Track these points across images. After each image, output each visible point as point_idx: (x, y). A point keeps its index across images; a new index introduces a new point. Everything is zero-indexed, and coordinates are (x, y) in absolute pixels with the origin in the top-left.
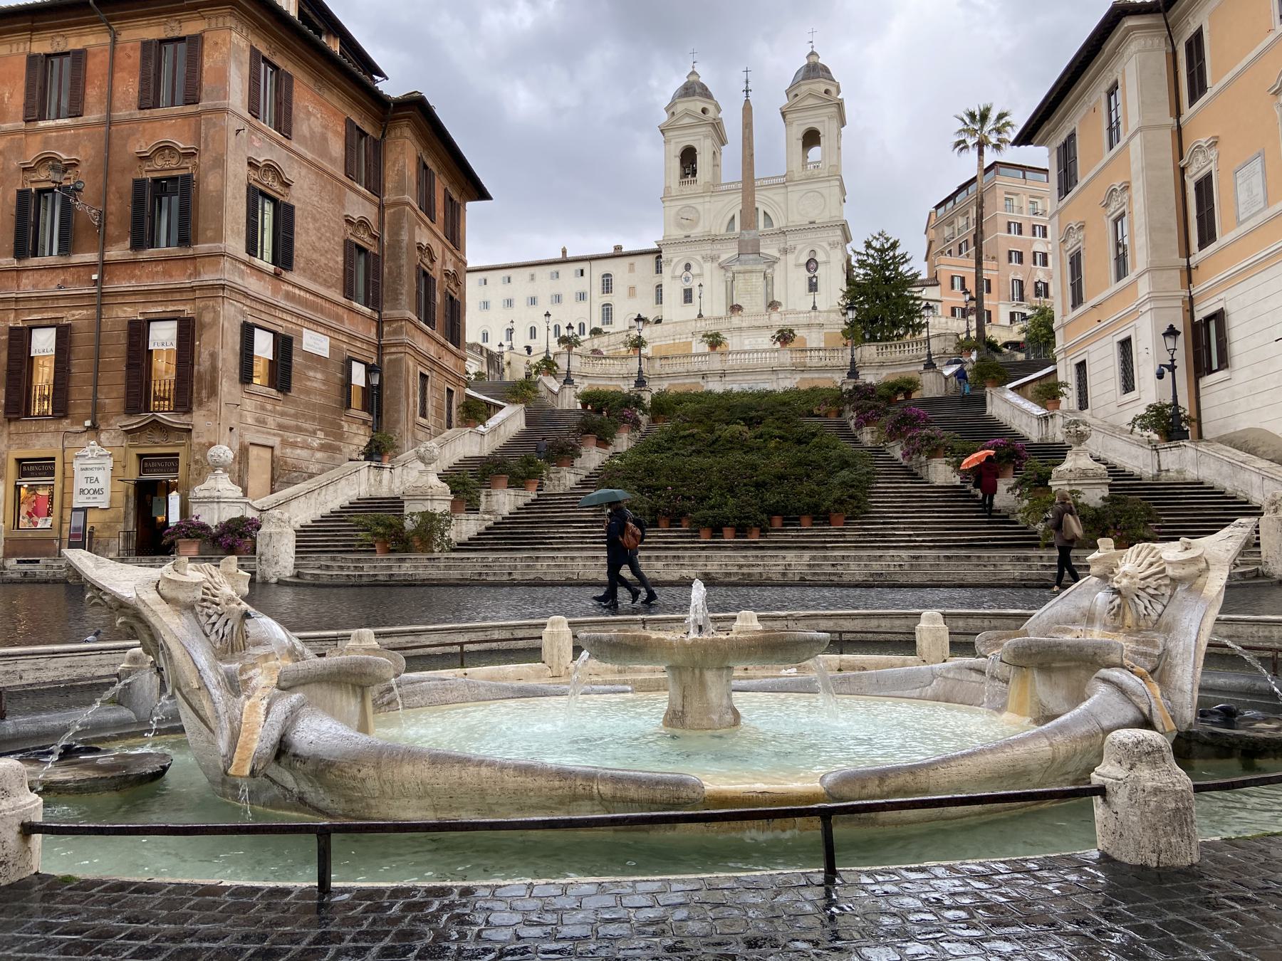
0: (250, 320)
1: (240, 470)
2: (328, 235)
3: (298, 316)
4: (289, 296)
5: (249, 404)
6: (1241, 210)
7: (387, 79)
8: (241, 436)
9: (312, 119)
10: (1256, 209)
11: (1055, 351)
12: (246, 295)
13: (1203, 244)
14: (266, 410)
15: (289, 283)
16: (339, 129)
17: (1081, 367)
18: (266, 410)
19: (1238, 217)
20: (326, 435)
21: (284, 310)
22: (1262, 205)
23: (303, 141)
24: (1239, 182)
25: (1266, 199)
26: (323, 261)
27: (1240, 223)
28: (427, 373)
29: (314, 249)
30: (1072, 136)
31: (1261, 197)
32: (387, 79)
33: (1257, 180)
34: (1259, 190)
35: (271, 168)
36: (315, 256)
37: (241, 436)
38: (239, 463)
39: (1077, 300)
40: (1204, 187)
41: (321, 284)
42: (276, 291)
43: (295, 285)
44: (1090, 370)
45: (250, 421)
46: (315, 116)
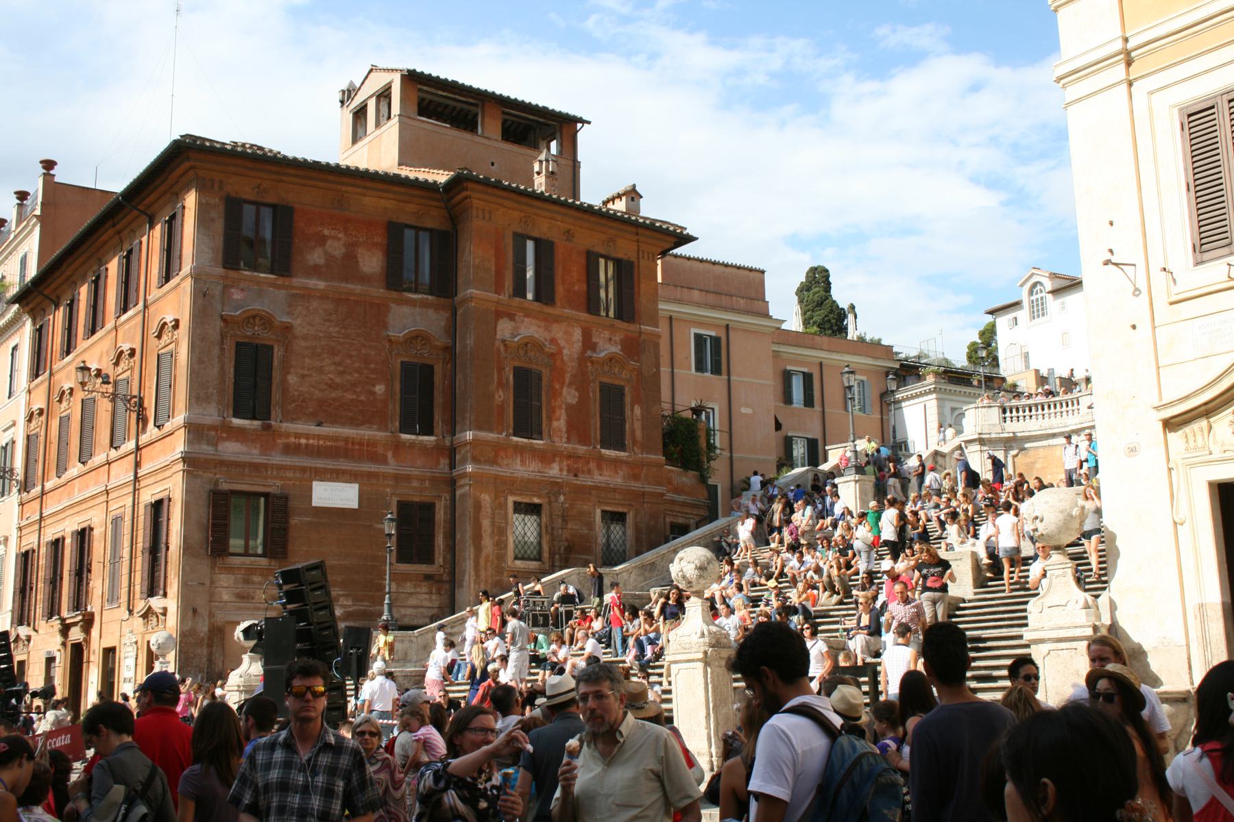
0: (225, 487)
1: (210, 654)
2: (356, 365)
3: (303, 470)
4: (288, 450)
5: (225, 580)
7: (589, 123)
8: (211, 615)
9: (329, 242)
12: (222, 463)
14: (254, 583)
15: (288, 435)
16: (378, 239)
18: (254, 583)
20: (357, 599)
21: (281, 468)
23: (315, 271)
26: (350, 396)
28: (536, 500)
29: (332, 386)
32: (589, 123)
35: (252, 318)
36: (333, 395)
37: (211, 615)
38: (210, 646)
41: (343, 424)
42: (265, 450)
43: (298, 436)
45: (226, 597)
46: (333, 238)
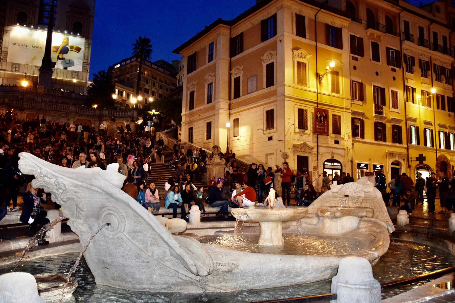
6: (249, 90)
10: (254, 90)
11: (181, 123)
13: (235, 98)
17: (191, 130)
19: (247, 91)
22: (255, 90)
24: (249, 81)
25: (257, 88)
27: (248, 93)
30: (195, 54)
31: (255, 88)
33: (255, 82)
34: (255, 85)
39: (191, 107)
40: (237, 80)
44: (194, 130)
